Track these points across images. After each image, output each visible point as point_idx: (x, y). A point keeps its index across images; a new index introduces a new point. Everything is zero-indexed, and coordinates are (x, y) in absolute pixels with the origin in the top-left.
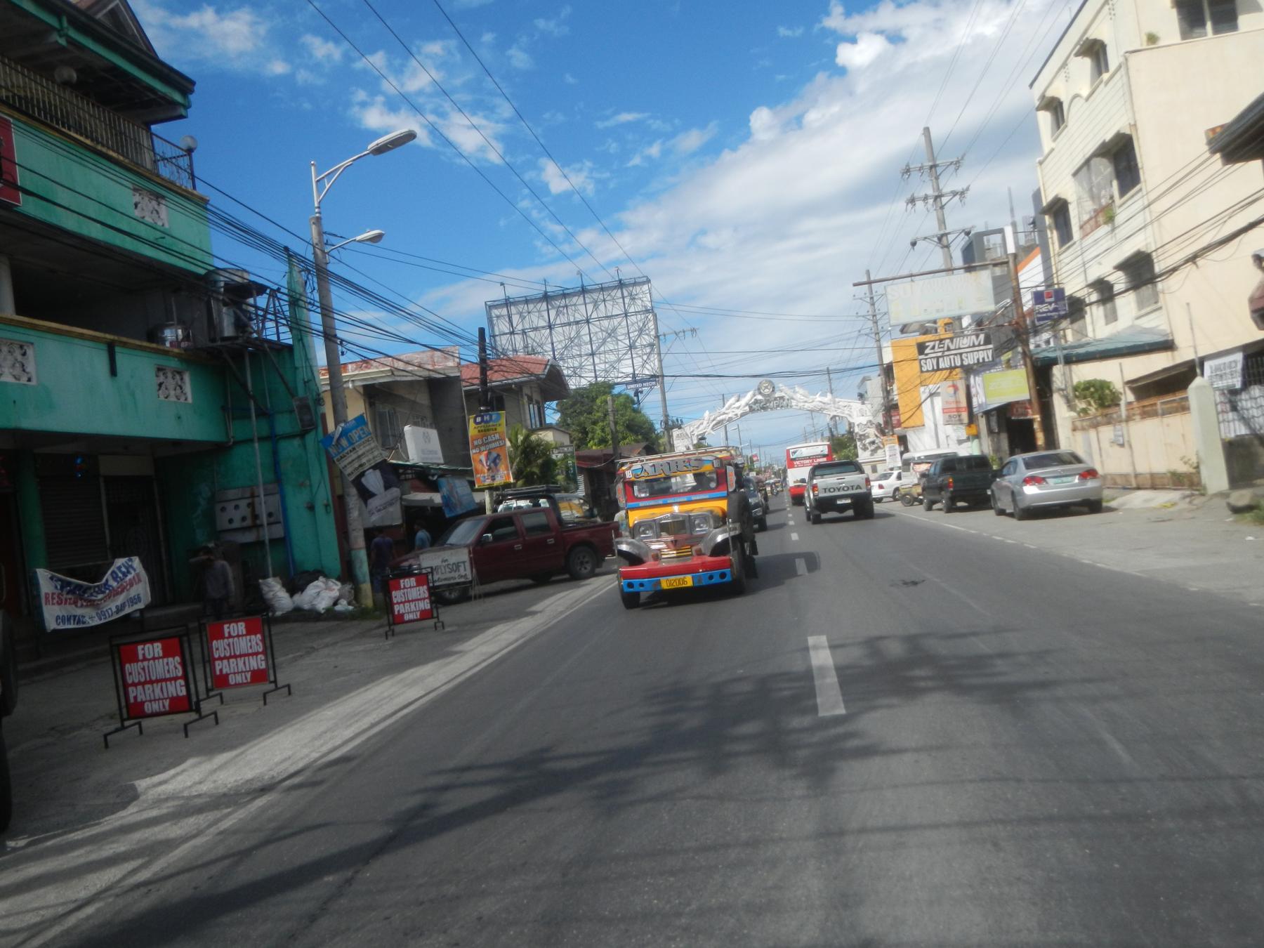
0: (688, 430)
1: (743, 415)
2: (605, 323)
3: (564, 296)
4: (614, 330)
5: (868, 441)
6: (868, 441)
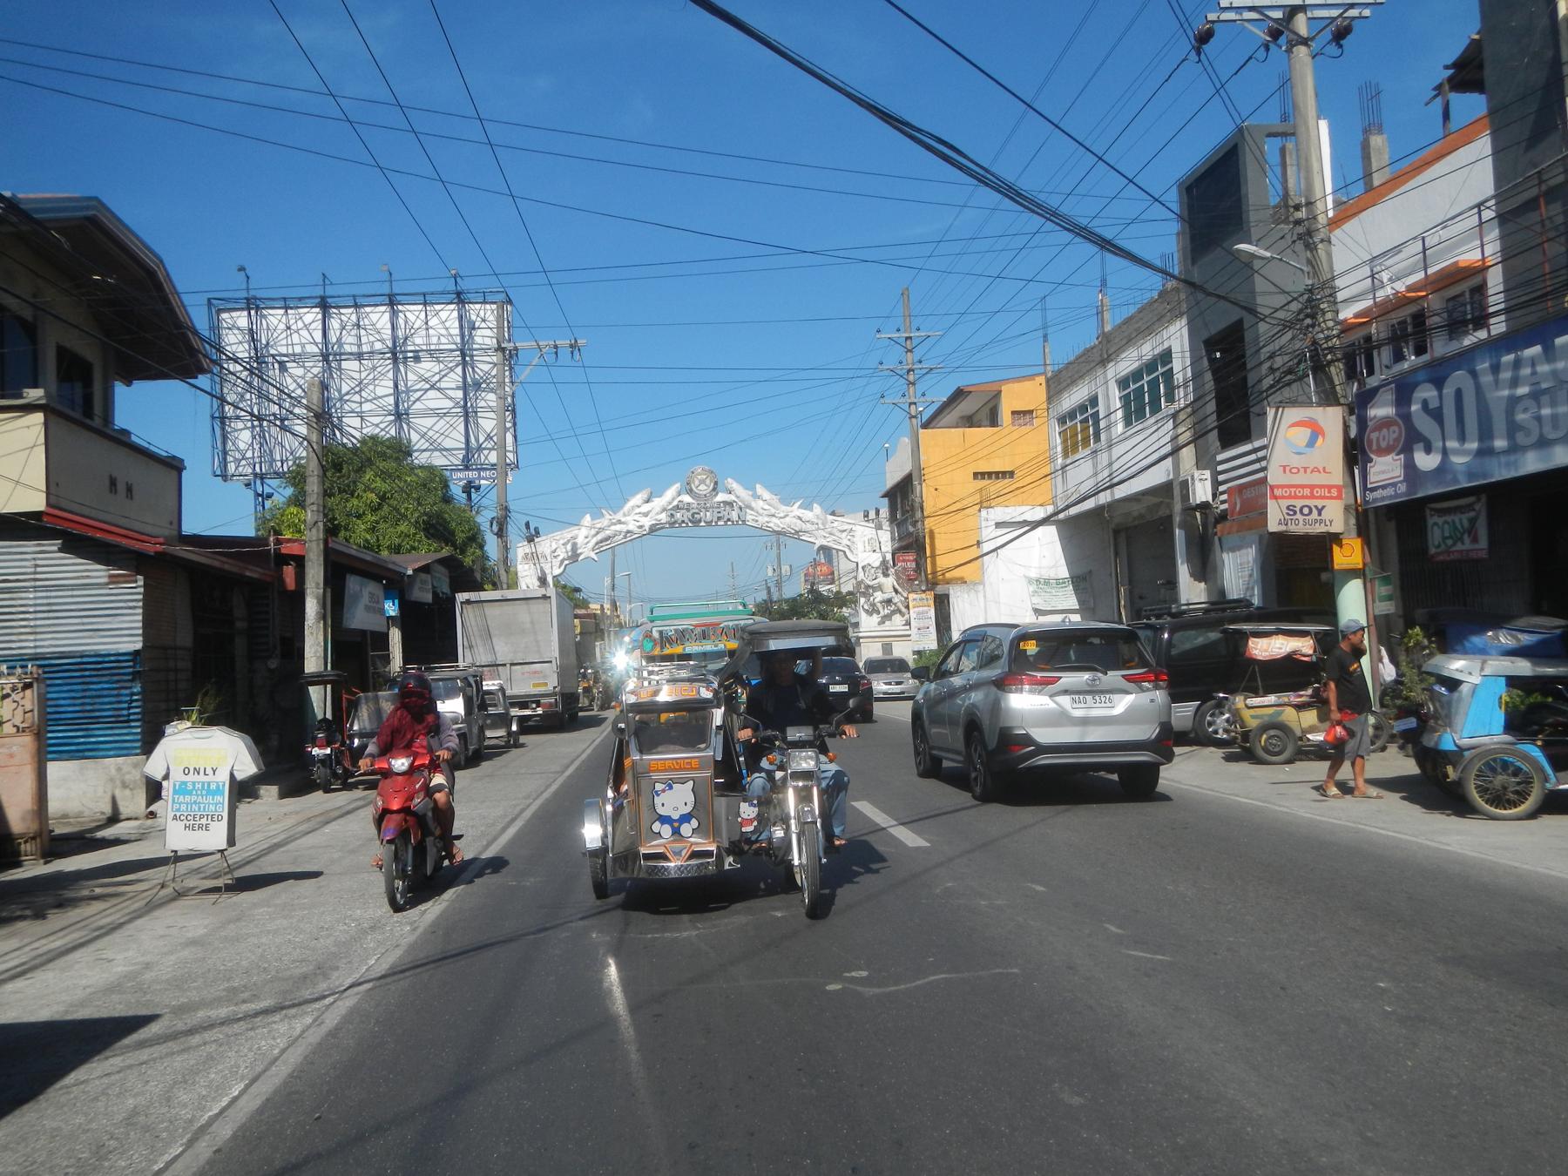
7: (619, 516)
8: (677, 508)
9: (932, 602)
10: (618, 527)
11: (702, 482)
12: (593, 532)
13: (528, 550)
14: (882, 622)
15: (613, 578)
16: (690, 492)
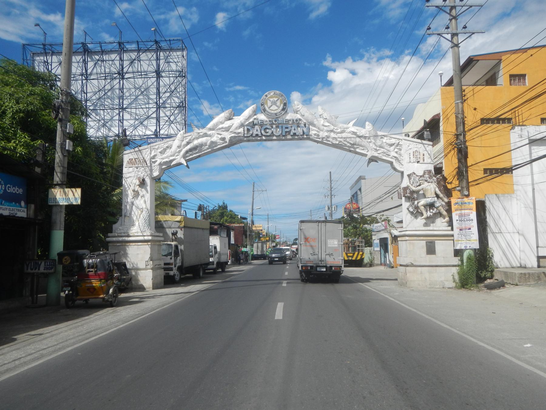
0: (147, 152)
1: (234, 142)
2: (140, 81)
3: (103, 52)
4: (147, 89)
5: (423, 202)
6: (423, 202)
8: (253, 125)
9: (474, 206)
11: (274, 103)
12: (184, 142)
13: (131, 157)
14: (426, 225)
15: (253, 209)
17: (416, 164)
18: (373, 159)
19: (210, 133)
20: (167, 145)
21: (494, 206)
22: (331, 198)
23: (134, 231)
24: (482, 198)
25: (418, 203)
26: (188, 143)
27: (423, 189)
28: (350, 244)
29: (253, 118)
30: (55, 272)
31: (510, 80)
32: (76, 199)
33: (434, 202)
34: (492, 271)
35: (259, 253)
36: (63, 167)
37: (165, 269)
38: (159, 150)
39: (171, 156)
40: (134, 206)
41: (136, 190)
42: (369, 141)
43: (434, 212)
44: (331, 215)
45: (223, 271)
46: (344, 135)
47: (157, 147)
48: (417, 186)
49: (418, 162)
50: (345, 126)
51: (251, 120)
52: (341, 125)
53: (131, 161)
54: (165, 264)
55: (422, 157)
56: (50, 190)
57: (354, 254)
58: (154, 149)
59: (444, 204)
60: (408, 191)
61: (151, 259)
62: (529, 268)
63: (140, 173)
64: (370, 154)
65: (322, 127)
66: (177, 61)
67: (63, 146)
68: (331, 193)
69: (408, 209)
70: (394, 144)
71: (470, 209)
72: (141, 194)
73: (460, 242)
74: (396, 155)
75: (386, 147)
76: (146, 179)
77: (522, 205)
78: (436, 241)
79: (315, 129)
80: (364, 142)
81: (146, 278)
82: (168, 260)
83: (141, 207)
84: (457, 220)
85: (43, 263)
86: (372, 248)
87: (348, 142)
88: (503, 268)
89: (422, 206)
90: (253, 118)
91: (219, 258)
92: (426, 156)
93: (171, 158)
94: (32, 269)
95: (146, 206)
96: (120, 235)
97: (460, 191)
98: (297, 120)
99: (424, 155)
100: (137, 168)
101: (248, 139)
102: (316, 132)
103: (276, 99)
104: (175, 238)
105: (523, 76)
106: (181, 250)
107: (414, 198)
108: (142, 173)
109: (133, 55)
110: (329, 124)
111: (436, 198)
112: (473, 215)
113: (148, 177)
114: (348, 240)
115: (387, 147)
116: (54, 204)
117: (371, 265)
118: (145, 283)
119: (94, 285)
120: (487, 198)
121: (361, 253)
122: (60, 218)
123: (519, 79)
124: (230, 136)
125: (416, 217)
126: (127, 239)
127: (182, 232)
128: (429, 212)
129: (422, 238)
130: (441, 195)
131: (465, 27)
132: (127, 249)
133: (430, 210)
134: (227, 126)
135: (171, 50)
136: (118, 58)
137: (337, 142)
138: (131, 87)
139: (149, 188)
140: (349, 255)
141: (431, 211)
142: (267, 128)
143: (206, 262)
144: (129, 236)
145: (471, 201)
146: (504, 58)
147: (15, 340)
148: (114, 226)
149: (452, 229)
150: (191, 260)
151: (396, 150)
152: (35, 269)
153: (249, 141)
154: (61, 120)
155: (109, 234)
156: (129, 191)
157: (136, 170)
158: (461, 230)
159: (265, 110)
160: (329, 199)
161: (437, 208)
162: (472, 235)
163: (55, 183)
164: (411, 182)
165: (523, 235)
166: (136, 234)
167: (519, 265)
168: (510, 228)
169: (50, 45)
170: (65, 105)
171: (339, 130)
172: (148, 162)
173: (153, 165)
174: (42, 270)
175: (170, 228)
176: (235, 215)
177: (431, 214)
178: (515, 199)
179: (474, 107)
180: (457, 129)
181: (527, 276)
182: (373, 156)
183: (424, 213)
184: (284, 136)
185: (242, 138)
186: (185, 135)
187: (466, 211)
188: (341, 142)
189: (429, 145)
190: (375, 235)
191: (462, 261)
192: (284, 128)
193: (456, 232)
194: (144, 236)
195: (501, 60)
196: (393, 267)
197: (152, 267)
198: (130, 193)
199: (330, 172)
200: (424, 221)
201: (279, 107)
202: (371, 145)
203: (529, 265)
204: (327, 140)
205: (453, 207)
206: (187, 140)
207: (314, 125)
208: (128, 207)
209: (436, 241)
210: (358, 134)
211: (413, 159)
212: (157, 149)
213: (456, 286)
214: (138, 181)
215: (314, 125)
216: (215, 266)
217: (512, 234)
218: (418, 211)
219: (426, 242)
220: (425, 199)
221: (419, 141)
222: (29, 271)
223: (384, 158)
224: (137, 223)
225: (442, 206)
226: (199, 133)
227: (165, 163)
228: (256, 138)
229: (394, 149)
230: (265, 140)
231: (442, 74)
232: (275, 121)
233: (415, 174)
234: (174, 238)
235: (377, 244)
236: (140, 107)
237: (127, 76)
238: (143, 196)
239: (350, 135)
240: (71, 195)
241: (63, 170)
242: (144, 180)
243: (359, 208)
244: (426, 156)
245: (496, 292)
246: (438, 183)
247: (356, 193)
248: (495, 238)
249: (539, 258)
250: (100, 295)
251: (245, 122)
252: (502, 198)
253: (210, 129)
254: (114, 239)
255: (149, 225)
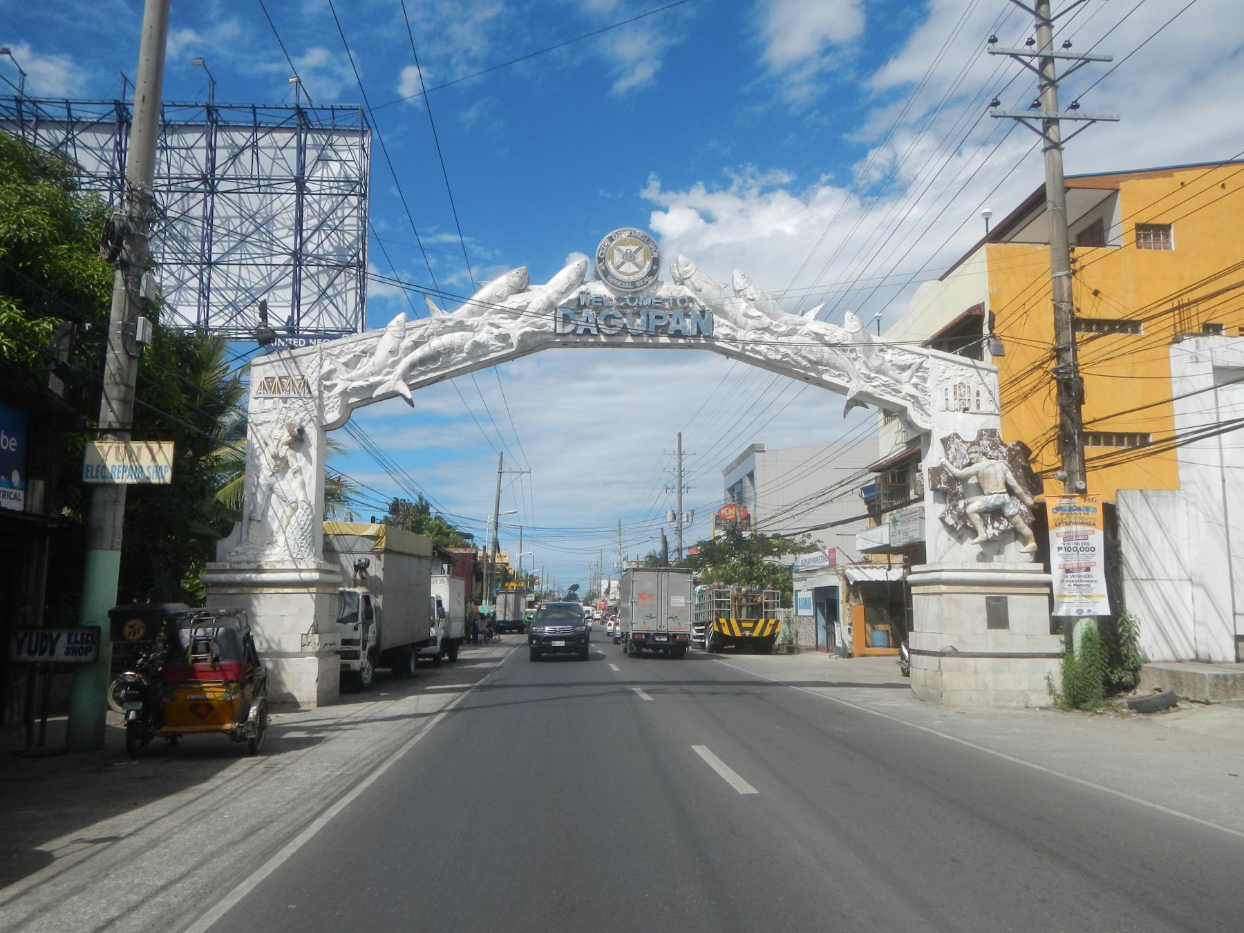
0: (311, 363)
1: (530, 345)
2: (253, 202)
4: (270, 219)
5: (977, 503)
6: (977, 503)
7: (461, 312)
8: (579, 306)
10: (454, 338)
11: (630, 257)
12: (407, 342)
13: (272, 373)
14: (983, 557)
15: (497, 515)
16: (603, 275)
17: (960, 415)
18: (860, 400)
19: (469, 322)
20: (363, 347)
21: (1139, 518)
22: (680, 493)
23: (273, 558)
24: (1111, 501)
25: (966, 506)
26: (416, 345)
27: (977, 474)
28: (744, 601)
29: (579, 290)
30: (96, 660)
31: (1138, 237)
32: (158, 469)
33: (1004, 504)
34: (1136, 669)
35: (509, 618)
36: (127, 386)
37: (345, 655)
38: (343, 359)
39: (373, 374)
40: (274, 496)
41: (281, 455)
42: (854, 355)
43: (1002, 527)
44: (679, 532)
45: (453, 659)
46: (794, 339)
47: (337, 350)
48: (964, 467)
49: (965, 410)
50: (797, 319)
51: (574, 295)
52: (787, 317)
53: (268, 384)
54: (345, 642)
55: (973, 397)
56: (89, 445)
57: (756, 623)
58: (329, 354)
59: (1024, 509)
60: (943, 478)
61: (316, 629)
62: (1219, 662)
63: (292, 414)
64: (855, 387)
65: (743, 320)
66: (348, 156)
67: (128, 330)
68: (680, 482)
69: (942, 519)
70: (909, 367)
71: (1089, 524)
72: (294, 464)
73: (1066, 600)
74: (914, 392)
75: (891, 373)
76: (307, 429)
77: (1201, 518)
78: (1009, 597)
79: (727, 322)
80: (841, 359)
81: (302, 677)
82: (348, 631)
83: (291, 498)
84: (1060, 549)
85: (64, 638)
86: (793, 610)
87: (804, 357)
88: (1158, 662)
89: (976, 512)
90: (579, 290)
91: (447, 628)
92: (985, 397)
93: (373, 380)
94: (31, 653)
95: (306, 496)
96: (236, 566)
97: (1064, 480)
98: (683, 301)
99: (978, 394)
100: (285, 400)
101: (564, 339)
102: (729, 331)
103: (634, 248)
104: (363, 578)
105: (1165, 228)
106: (377, 608)
107: (956, 494)
108: (298, 413)
109: (241, 138)
110: (759, 313)
111: (1007, 496)
112: (1097, 539)
113: (312, 424)
114: (739, 590)
115: (895, 373)
116: (100, 480)
117: (791, 650)
118: (300, 690)
119: (209, 696)
120: (1121, 499)
121: (772, 621)
122: (112, 520)
123: (1157, 235)
124: (522, 331)
125: (960, 539)
126: (254, 577)
127: (381, 564)
128: (990, 527)
129: (977, 589)
130: (1019, 489)
131: (1075, 106)
132: (255, 602)
133: (992, 523)
134: (514, 306)
135: (335, 130)
136: (203, 142)
137: (779, 357)
138: (231, 212)
139: (313, 451)
140: (744, 625)
141: (996, 524)
142: (612, 317)
143: (423, 637)
144: (259, 570)
145: (1093, 505)
146: (1122, 185)
147: (47, 859)
148: (223, 545)
149: (1047, 570)
150: (395, 636)
151: (914, 380)
152: (42, 653)
153: (565, 345)
154: (124, 266)
155: (209, 565)
156: (262, 458)
157: (281, 404)
158: (1068, 571)
159: (606, 273)
160: (675, 496)
161: (1009, 518)
162: (1092, 585)
163: (101, 426)
164: (951, 456)
165: (1202, 586)
166: (279, 566)
167: (1193, 656)
168: (1173, 570)
169: (34, 103)
170: (137, 226)
171: (784, 329)
172: (314, 388)
173: (326, 394)
174: (60, 653)
175: (350, 552)
176: (449, 527)
177: (997, 533)
178: (1183, 502)
179: (1094, 287)
180: (1057, 336)
181: (1230, 683)
182: (861, 393)
183: (980, 528)
184: (650, 336)
185: (549, 337)
186: (409, 325)
187: (1079, 528)
188: (787, 355)
189: (990, 371)
190: (799, 580)
191: (1069, 643)
192: (652, 317)
193: (1056, 576)
194: (301, 571)
195: (1117, 190)
196: (850, 656)
197: (317, 648)
198: (265, 462)
199: (680, 435)
200: (979, 549)
201: (640, 267)
202: (857, 365)
203: (1217, 656)
204: (753, 350)
205: (1051, 517)
206: (414, 337)
207: (725, 315)
208: (259, 498)
209: (1009, 597)
210: (827, 338)
211: (953, 404)
212: (338, 356)
213: (1055, 704)
214: (287, 434)
215: (725, 315)
216: (437, 648)
217: (1176, 583)
218: (965, 526)
219: (987, 599)
220: (982, 498)
221: (968, 360)
222: (25, 656)
223: (887, 397)
224: (280, 539)
225: (1021, 514)
226: (443, 322)
227: (357, 391)
228: (584, 339)
229: (911, 378)
230: (605, 345)
231: (990, 214)
232: (632, 298)
233: (958, 437)
234: (358, 577)
235: (806, 600)
236: (250, 262)
237: (222, 186)
238: (298, 471)
239: (808, 340)
240: (145, 460)
241: (126, 395)
242: (301, 431)
243: (748, 517)
244: (985, 397)
245: (1157, 718)
246: (1012, 461)
247: (741, 481)
248: (1141, 591)
249: (1239, 639)
250: (223, 723)
251: (558, 299)
252: (1153, 500)
253: (472, 313)
254: (222, 577)
255: (313, 544)
